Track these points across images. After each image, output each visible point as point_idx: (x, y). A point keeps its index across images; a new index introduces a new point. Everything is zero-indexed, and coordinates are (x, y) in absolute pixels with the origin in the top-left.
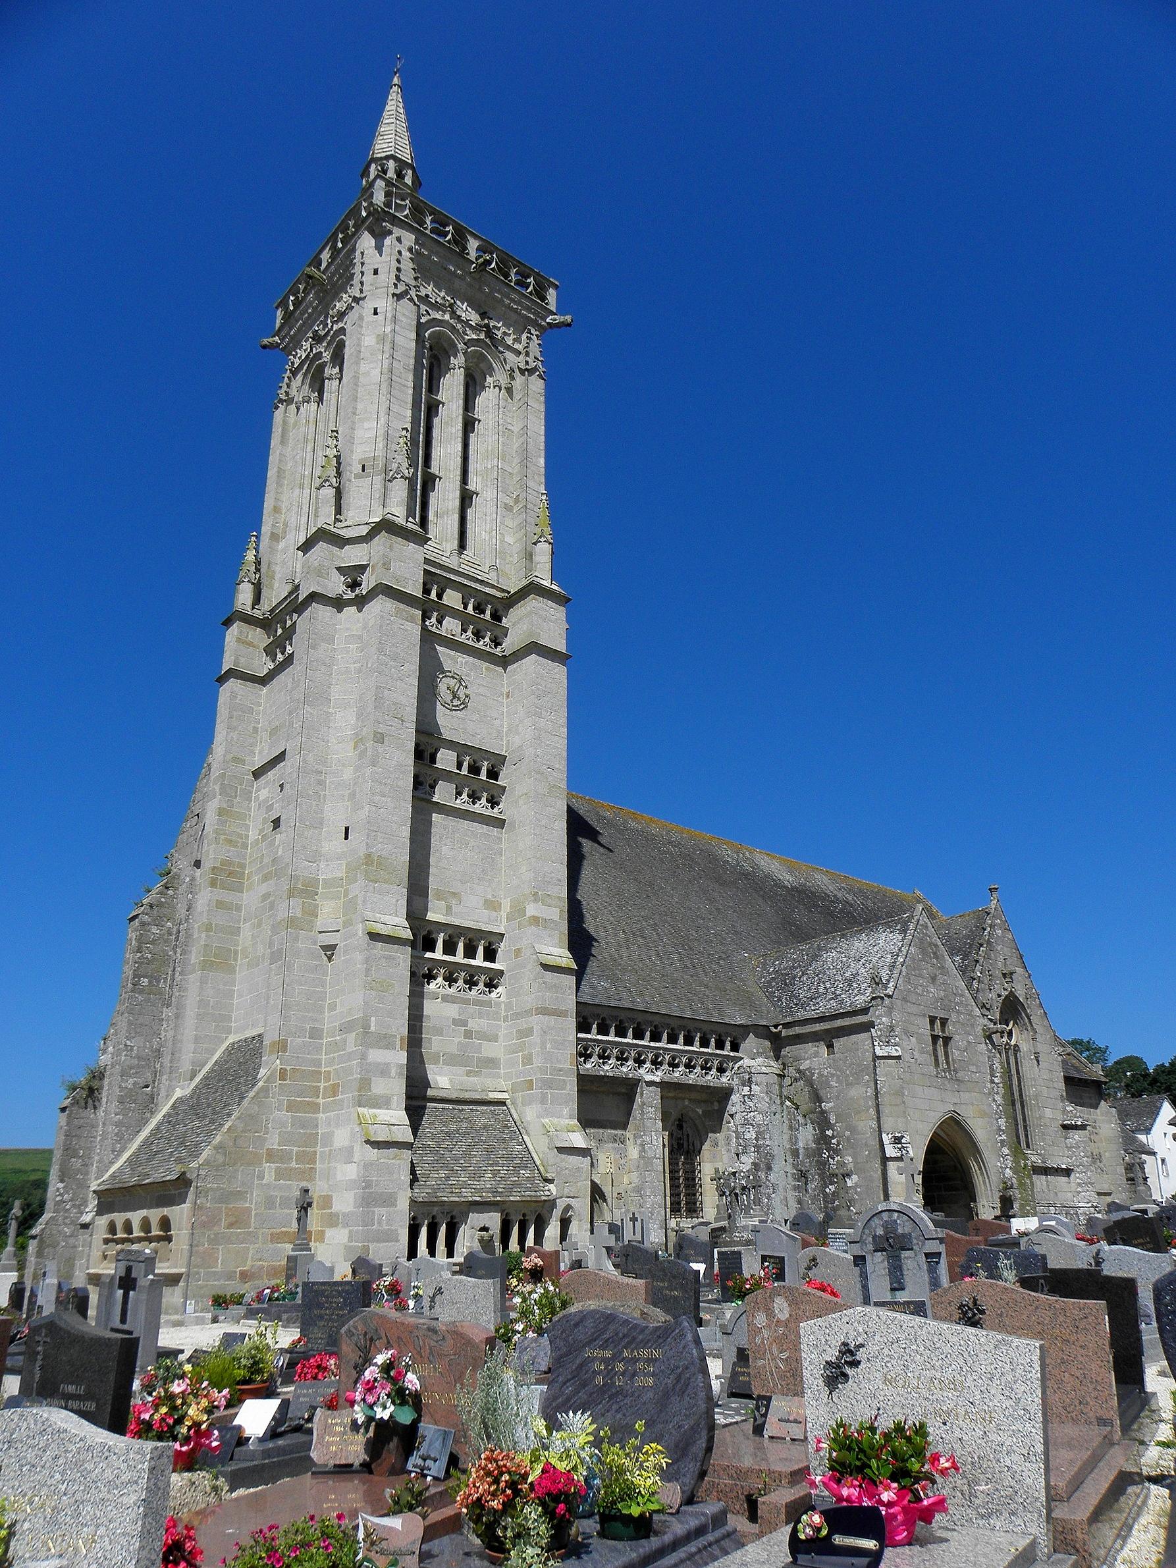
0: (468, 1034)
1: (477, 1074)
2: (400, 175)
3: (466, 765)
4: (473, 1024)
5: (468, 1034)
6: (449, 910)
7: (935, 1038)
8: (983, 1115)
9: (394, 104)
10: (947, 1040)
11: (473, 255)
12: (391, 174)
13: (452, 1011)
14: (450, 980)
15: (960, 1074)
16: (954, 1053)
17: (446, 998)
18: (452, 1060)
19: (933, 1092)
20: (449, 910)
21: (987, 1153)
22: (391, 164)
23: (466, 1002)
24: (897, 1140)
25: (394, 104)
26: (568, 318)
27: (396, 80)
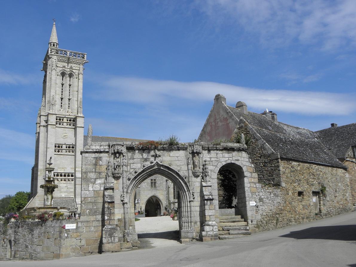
0: (68, 188)
1: (69, 194)
2: (54, 45)
3: (68, 147)
4: (68, 187)
5: (68, 188)
6: (64, 170)
7: (152, 183)
8: (162, 195)
9: (54, 29)
10: (155, 183)
11: (68, 55)
12: (52, 46)
13: (65, 185)
14: (65, 180)
15: (157, 188)
16: (157, 185)
17: (64, 183)
18: (65, 192)
19: (150, 192)
20: (64, 170)
21: (162, 201)
22: (52, 44)
23: (68, 183)
24: (138, 200)
25: (54, 29)
26: (88, 61)
27: (54, 23)
